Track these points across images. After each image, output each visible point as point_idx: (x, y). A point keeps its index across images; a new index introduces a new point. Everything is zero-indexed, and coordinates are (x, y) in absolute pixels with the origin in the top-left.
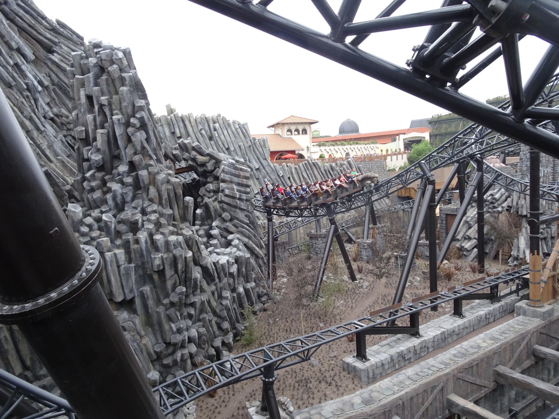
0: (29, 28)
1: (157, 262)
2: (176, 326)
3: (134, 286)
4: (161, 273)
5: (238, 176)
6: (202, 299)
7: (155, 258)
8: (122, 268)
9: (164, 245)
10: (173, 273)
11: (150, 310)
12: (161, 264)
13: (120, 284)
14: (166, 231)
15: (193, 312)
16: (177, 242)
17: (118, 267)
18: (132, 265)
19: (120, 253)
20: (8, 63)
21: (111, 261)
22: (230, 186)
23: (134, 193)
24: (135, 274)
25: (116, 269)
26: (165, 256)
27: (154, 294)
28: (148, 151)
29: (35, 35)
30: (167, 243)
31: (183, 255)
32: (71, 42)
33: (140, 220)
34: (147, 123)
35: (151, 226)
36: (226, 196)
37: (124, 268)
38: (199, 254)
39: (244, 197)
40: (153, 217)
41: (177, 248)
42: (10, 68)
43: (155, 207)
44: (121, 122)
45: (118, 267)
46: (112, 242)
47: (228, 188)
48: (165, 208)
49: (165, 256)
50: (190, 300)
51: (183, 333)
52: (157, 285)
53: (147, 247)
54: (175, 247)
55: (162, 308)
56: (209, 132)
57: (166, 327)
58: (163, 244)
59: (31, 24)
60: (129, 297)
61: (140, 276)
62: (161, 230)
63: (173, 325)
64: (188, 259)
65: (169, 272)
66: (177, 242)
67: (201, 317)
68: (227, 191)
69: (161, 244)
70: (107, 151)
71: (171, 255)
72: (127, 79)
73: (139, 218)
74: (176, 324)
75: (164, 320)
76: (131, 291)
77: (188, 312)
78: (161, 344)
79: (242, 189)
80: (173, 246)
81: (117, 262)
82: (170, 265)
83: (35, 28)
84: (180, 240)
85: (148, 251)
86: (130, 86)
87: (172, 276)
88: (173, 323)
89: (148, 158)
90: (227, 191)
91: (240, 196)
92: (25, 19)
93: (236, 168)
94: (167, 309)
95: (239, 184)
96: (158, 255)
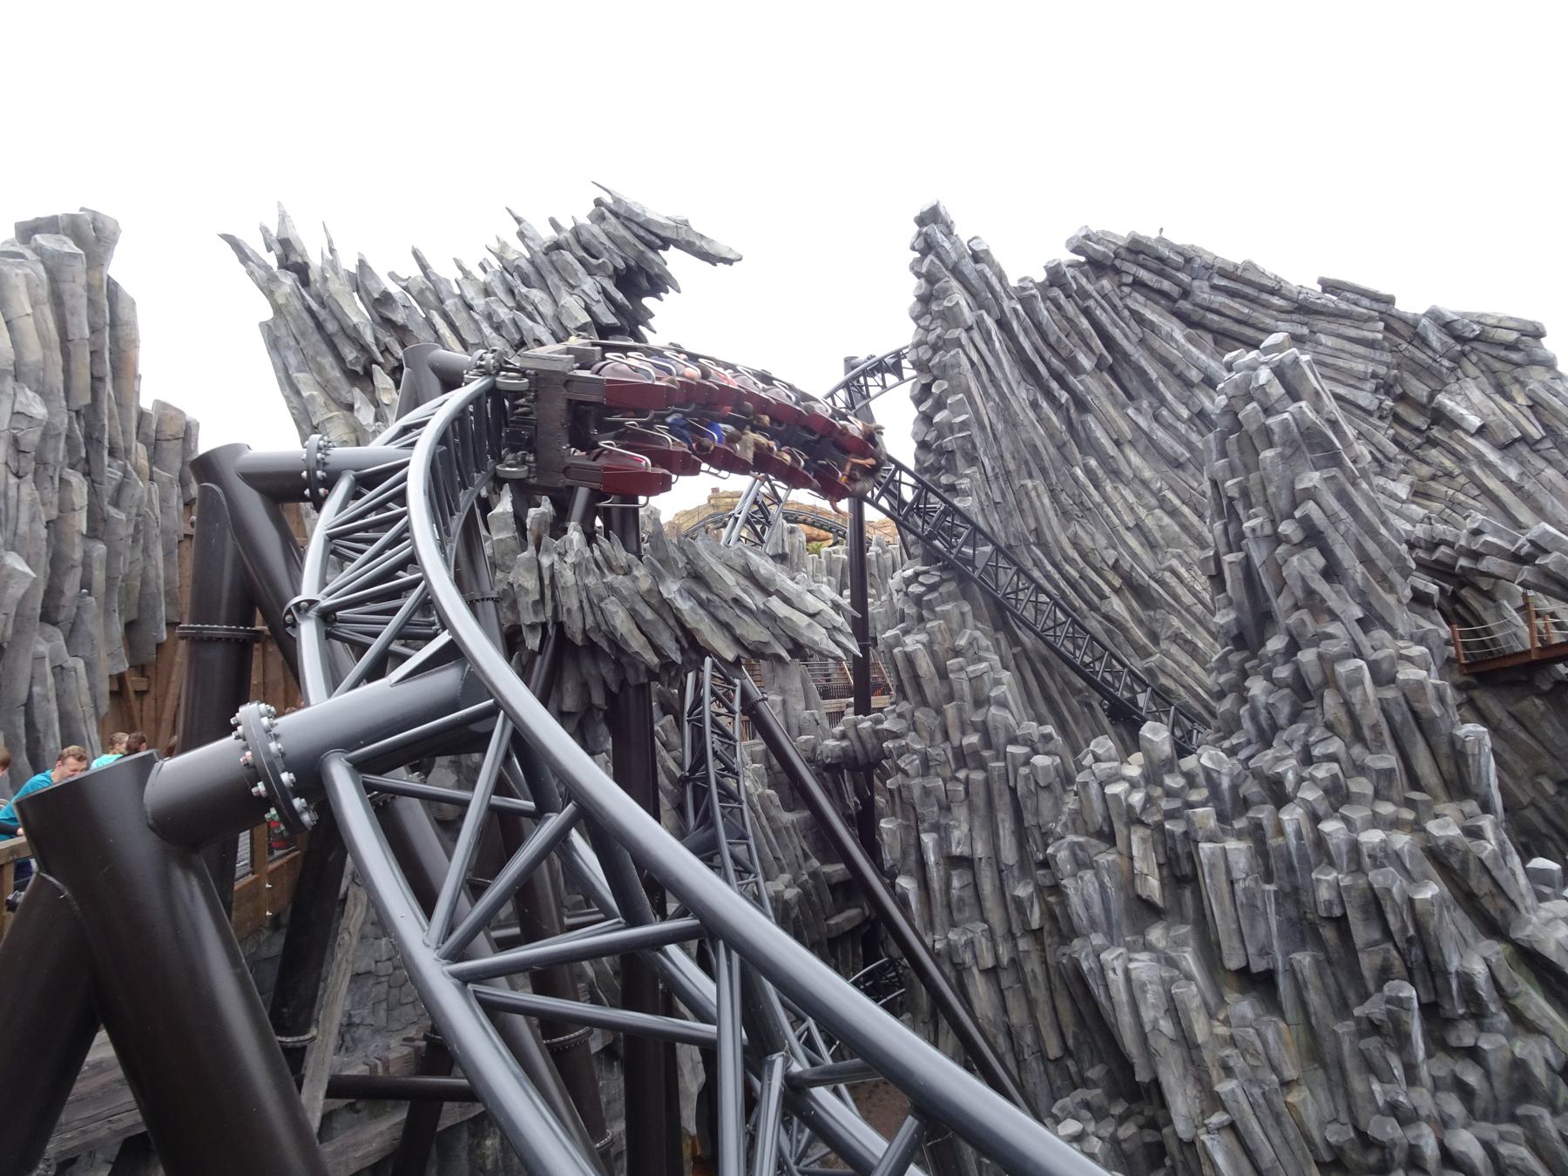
0: (1236, 328)
1: (1324, 894)
2: (1385, 1093)
3: (1275, 943)
4: (1341, 923)
6: (1517, 1051)
7: (1318, 880)
8: (1239, 887)
9: (1348, 852)
10: (1376, 935)
11: (1313, 1020)
12: (1336, 901)
13: (1234, 926)
14: (1358, 813)
15: (1472, 1077)
16: (1384, 850)
17: (1232, 883)
18: (1271, 888)
19: (1237, 848)
20: (1178, 418)
21: (1212, 866)
23: (1294, 704)
24: (1278, 913)
25: (1225, 887)
26: (1346, 881)
27: (1330, 981)
28: (1323, 601)
29: (1250, 338)
30: (1355, 847)
31: (1395, 890)
32: (1348, 322)
33: (1290, 776)
34: (1322, 529)
35: (1310, 794)
37: (1245, 890)
38: (1502, 903)
40: (1322, 772)
41: (1383, 866)
42: (1182, 428)
43: (1336, 746)
44: (1259, 533)
45: (1232, 883)
46: (1222, 818)
48: (1374, 750)
49: (1346, 881)
50: (1459, 1038)
51: (1419, 1127)
52: (1335, 956)
53: (1300, 847)
54: (1377, 864)
55: (1348, 1026)
58: (1344, 849)
59: (1240, 317)
60: (1258, 966)
61: (1289, 920)
62: (1344, 810)
63: (1376, 1087)
64: (1418, 906)
65: (1362, 933)
66: (1384, 850)
67: (1521, 1110)
69: (1338, 846)
70: (1246, 603)
71: (1361, 882)
72: (1276, 429)
73: (1287, 771)
74: (1388, 1087)
75: (1351, 1064)
76: (1264, 951)
77: (1453, 1071)
78: (1345, 1128)
80: (1367, 859)
81: (1228, 871)
82: (1364, 909)
83: (1251, 321)
84: (1398, 847)
85: (1304, 858)
86: (1283, 444)
87: (1376, 943)
88: (1381, 1081)
89: (1327, 618)
92: (1228, 312)
94: (1361, 1035)
96: (1327, 875)
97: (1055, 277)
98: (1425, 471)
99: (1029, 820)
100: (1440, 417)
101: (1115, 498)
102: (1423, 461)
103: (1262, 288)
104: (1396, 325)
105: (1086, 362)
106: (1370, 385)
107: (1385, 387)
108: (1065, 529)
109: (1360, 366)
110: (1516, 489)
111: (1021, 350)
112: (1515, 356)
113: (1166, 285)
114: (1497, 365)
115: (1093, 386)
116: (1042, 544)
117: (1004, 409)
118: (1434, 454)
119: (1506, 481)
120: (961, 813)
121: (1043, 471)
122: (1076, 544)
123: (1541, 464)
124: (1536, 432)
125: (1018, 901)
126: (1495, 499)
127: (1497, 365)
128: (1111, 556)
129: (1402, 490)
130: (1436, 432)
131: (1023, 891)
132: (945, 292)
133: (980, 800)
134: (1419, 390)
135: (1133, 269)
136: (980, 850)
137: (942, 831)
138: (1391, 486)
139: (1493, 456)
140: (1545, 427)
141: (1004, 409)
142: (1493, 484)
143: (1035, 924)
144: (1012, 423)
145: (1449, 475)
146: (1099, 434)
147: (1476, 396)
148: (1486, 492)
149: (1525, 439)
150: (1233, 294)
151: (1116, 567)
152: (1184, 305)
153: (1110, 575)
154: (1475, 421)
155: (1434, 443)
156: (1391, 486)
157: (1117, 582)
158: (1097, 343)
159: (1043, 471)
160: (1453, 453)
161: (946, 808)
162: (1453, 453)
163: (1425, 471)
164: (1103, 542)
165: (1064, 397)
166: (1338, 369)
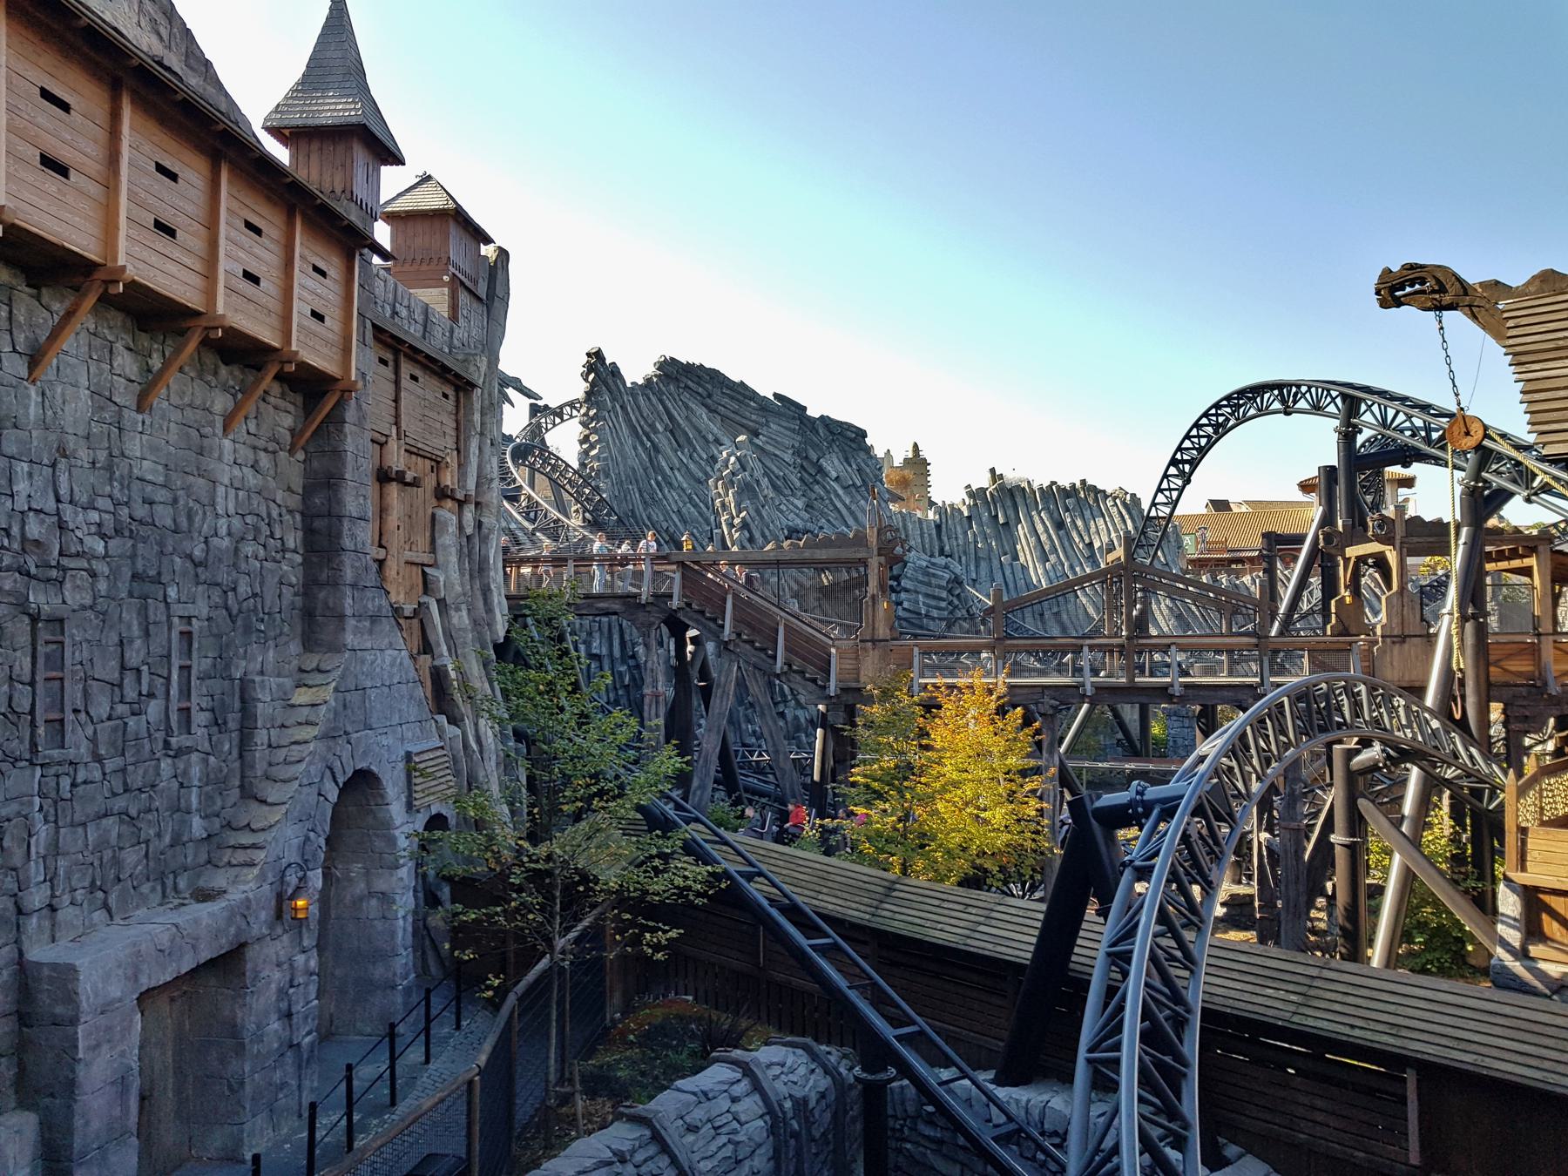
0: (732, 415)
5: (929, 584)
20: (701, 458)
22: (913, 596)
36: (904, 609)
39: (935, 613)
42: (703, 463)
47: (909, 600)
56: (1056, 515)
57: (744, 726)
68: (906, 605)
75: (742, 719)
79: (933, 603)
90: (906, 605)
91: (928, 611)
93: (928, 574)
94: (746, 709)
95: (927, 595)
97: (648, 381)
98: (813, 496)
99: (627, 637)
100: (821, 470)
101: (669, 497)
102: (812, 490)
103: (745, 397)
104: (805, 421)
105: (660, 428)
106: (790, 452)
107: (797, 453)
108: (645, 510)
109: (787, 442)
110: (848, 508)
111: (630, 420)
112: (853, 445)
113: (700, 390)
114: (847, 448)
115: (663, 440)
116: (634, 516)
117: (621, 451)
118: (816, 487)
119: (845, 504)
120: (597, 635)
121: (637, 481)
122: (649, 518)
123: (859, 498)
124: (859, 483)
125: (620, 673)
126: (839, 512)
127: (847, 448)
128: (665, 525)
129: (800, 504)
130: (818, 477)
131: (623, 668)
132: (600, 393)
133: (606, 630)
134: (813, 456)
135: (685, 380)
136: (605, 651)
137: (588, 644)
138: (796, 501)
139: (840, 492)
140: (863, 481)
141: (621, 451)
142: (839, 505)
143: (626, 682)
144: (624, 458)
145: (822, 499)
146: (664, 464)
147: (836, 462)
148: (836, 508)
149: (854, 485)
150: (732, 398)
151: (667, 531)
152: (709, 401)
153: (664, 535)
154: (834, 475)
155: (818, 483)
156: (796, 501)
157: (667, 538)
158: (665, 417)
159: (637, 481)
160: (824, 487)
161: (590, 634)
162: (824, 487)
163: (813, 496)
164: (662, 518)
165: (649, 444)
166: (777, 442)
